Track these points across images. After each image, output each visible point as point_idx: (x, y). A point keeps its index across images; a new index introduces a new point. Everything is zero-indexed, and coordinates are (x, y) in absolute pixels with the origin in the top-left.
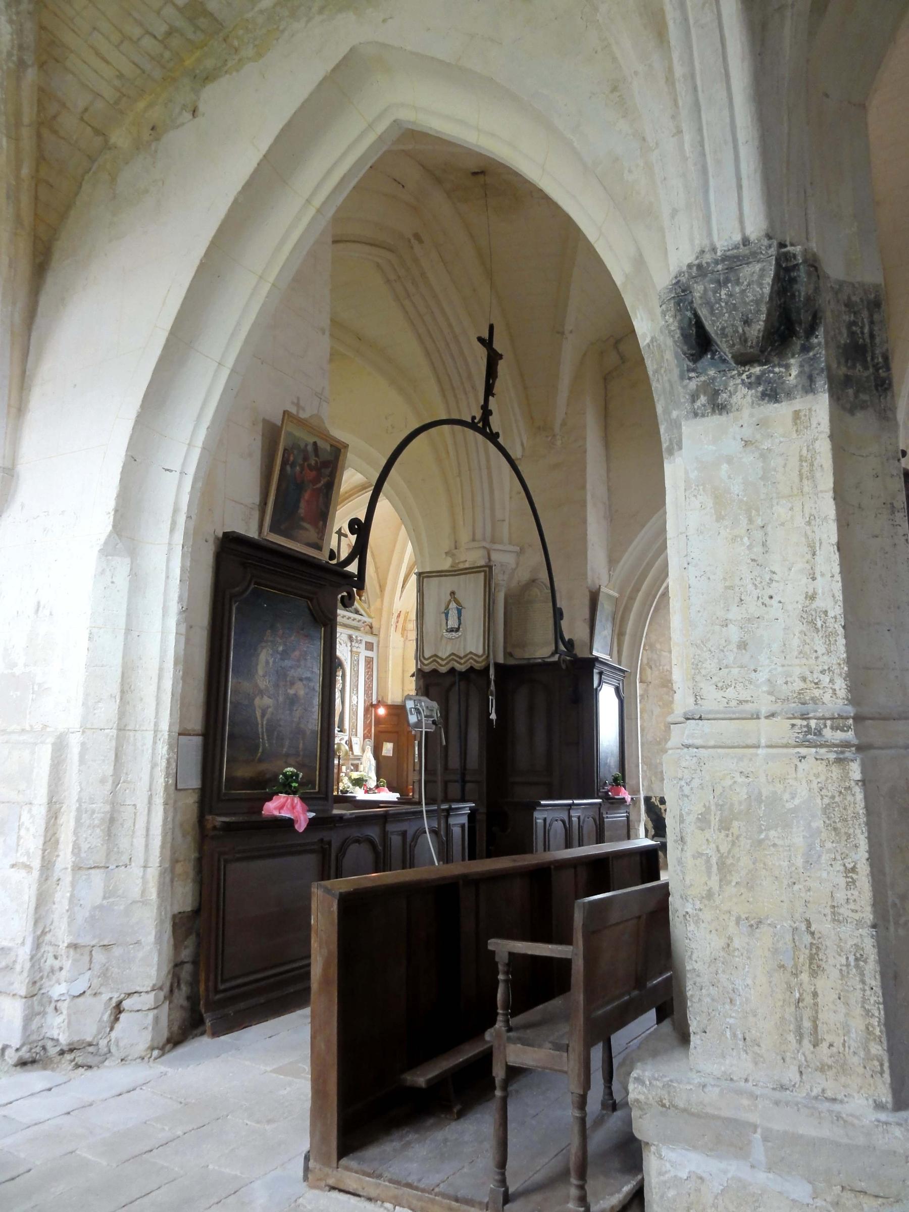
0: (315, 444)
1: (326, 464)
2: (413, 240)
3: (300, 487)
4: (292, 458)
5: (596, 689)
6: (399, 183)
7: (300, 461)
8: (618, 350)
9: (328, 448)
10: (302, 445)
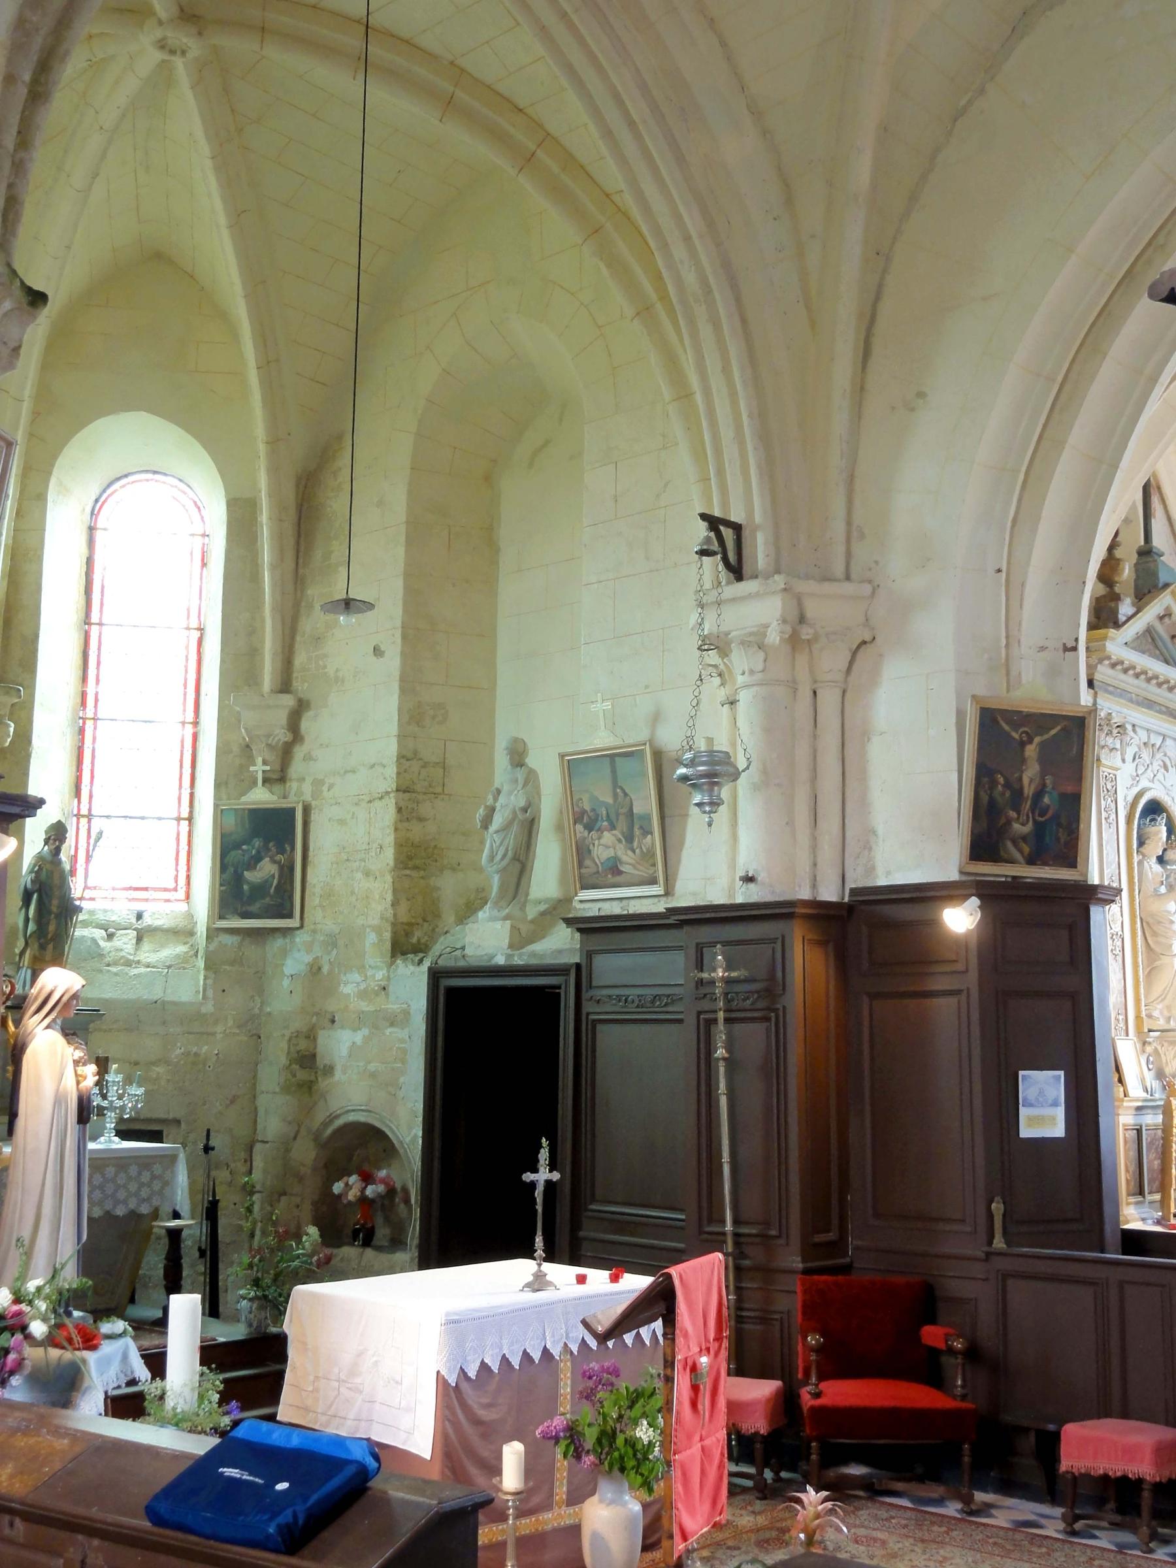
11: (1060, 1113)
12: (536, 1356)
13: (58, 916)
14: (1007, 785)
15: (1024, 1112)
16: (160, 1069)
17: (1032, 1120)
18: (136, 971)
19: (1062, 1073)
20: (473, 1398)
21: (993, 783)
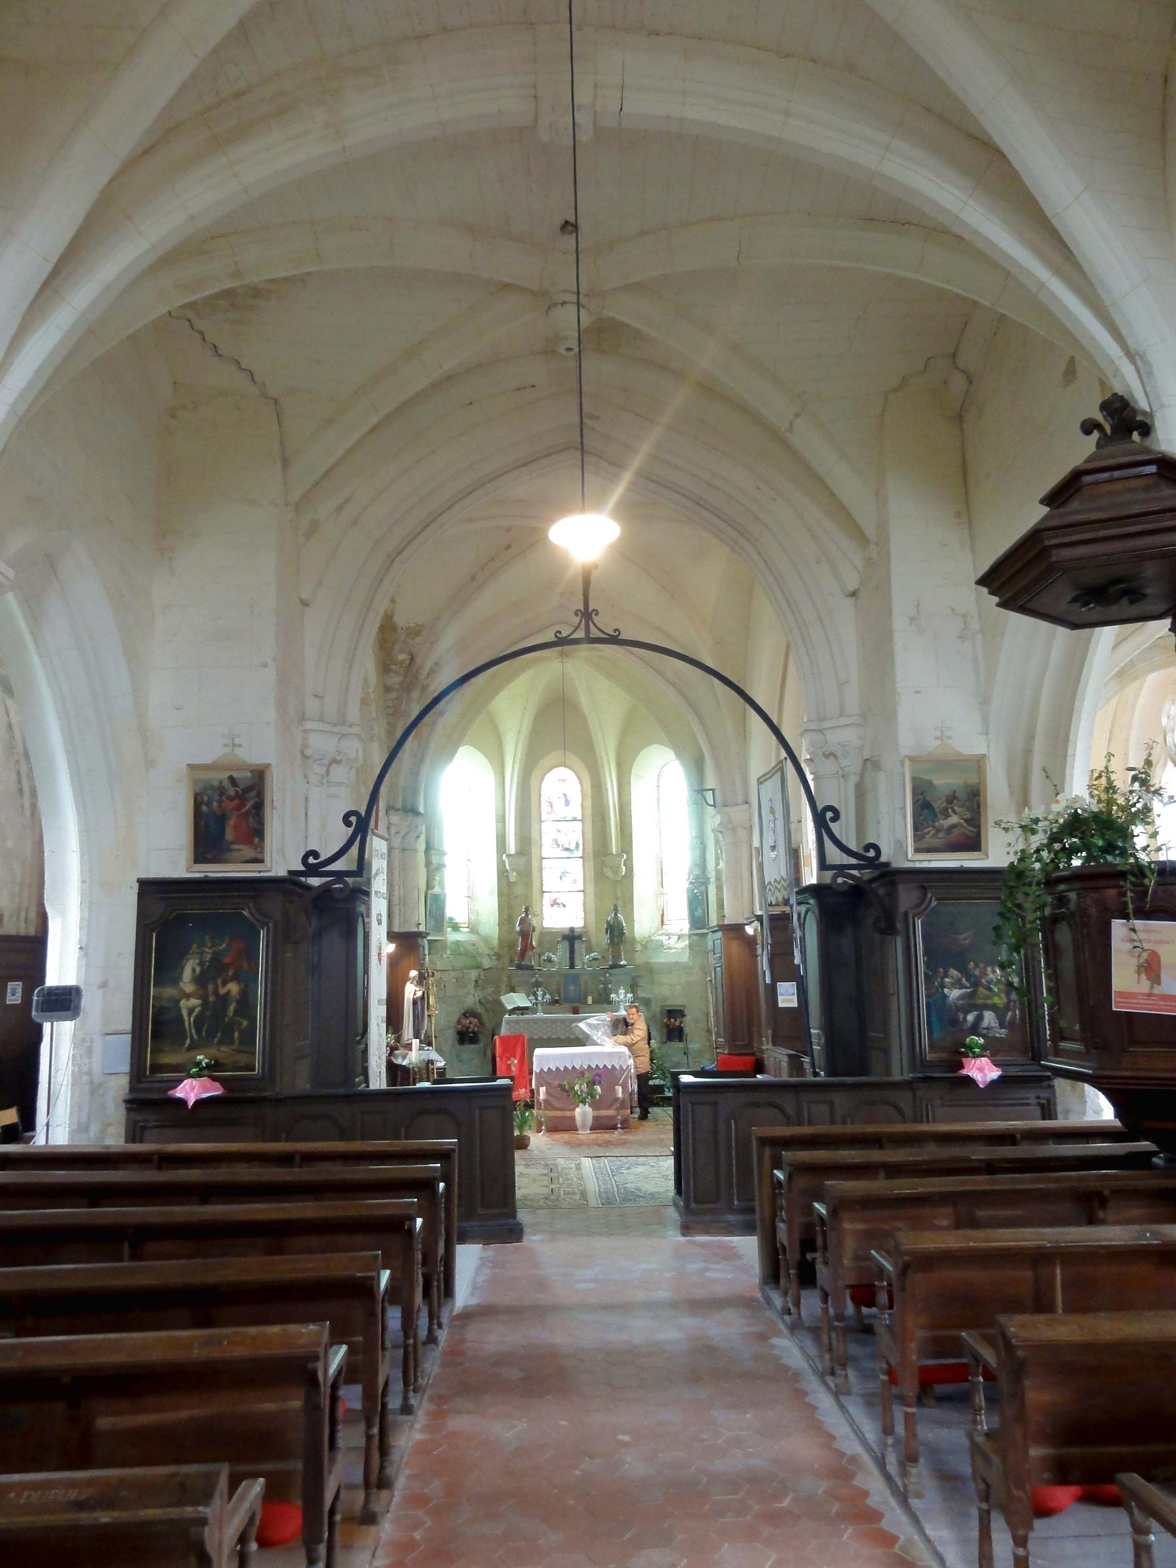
1: (249, 789)
3: (222, 819)
4: (206, 799)
5: (906, 914)
6: (525, 388)
7: (217, 797)
8: (958, 368)
9: (249, 775)
10: (216, 784)
15: (780, 998)
16: (678, 987)
17: (783, 1001)
20: (545, 1076)
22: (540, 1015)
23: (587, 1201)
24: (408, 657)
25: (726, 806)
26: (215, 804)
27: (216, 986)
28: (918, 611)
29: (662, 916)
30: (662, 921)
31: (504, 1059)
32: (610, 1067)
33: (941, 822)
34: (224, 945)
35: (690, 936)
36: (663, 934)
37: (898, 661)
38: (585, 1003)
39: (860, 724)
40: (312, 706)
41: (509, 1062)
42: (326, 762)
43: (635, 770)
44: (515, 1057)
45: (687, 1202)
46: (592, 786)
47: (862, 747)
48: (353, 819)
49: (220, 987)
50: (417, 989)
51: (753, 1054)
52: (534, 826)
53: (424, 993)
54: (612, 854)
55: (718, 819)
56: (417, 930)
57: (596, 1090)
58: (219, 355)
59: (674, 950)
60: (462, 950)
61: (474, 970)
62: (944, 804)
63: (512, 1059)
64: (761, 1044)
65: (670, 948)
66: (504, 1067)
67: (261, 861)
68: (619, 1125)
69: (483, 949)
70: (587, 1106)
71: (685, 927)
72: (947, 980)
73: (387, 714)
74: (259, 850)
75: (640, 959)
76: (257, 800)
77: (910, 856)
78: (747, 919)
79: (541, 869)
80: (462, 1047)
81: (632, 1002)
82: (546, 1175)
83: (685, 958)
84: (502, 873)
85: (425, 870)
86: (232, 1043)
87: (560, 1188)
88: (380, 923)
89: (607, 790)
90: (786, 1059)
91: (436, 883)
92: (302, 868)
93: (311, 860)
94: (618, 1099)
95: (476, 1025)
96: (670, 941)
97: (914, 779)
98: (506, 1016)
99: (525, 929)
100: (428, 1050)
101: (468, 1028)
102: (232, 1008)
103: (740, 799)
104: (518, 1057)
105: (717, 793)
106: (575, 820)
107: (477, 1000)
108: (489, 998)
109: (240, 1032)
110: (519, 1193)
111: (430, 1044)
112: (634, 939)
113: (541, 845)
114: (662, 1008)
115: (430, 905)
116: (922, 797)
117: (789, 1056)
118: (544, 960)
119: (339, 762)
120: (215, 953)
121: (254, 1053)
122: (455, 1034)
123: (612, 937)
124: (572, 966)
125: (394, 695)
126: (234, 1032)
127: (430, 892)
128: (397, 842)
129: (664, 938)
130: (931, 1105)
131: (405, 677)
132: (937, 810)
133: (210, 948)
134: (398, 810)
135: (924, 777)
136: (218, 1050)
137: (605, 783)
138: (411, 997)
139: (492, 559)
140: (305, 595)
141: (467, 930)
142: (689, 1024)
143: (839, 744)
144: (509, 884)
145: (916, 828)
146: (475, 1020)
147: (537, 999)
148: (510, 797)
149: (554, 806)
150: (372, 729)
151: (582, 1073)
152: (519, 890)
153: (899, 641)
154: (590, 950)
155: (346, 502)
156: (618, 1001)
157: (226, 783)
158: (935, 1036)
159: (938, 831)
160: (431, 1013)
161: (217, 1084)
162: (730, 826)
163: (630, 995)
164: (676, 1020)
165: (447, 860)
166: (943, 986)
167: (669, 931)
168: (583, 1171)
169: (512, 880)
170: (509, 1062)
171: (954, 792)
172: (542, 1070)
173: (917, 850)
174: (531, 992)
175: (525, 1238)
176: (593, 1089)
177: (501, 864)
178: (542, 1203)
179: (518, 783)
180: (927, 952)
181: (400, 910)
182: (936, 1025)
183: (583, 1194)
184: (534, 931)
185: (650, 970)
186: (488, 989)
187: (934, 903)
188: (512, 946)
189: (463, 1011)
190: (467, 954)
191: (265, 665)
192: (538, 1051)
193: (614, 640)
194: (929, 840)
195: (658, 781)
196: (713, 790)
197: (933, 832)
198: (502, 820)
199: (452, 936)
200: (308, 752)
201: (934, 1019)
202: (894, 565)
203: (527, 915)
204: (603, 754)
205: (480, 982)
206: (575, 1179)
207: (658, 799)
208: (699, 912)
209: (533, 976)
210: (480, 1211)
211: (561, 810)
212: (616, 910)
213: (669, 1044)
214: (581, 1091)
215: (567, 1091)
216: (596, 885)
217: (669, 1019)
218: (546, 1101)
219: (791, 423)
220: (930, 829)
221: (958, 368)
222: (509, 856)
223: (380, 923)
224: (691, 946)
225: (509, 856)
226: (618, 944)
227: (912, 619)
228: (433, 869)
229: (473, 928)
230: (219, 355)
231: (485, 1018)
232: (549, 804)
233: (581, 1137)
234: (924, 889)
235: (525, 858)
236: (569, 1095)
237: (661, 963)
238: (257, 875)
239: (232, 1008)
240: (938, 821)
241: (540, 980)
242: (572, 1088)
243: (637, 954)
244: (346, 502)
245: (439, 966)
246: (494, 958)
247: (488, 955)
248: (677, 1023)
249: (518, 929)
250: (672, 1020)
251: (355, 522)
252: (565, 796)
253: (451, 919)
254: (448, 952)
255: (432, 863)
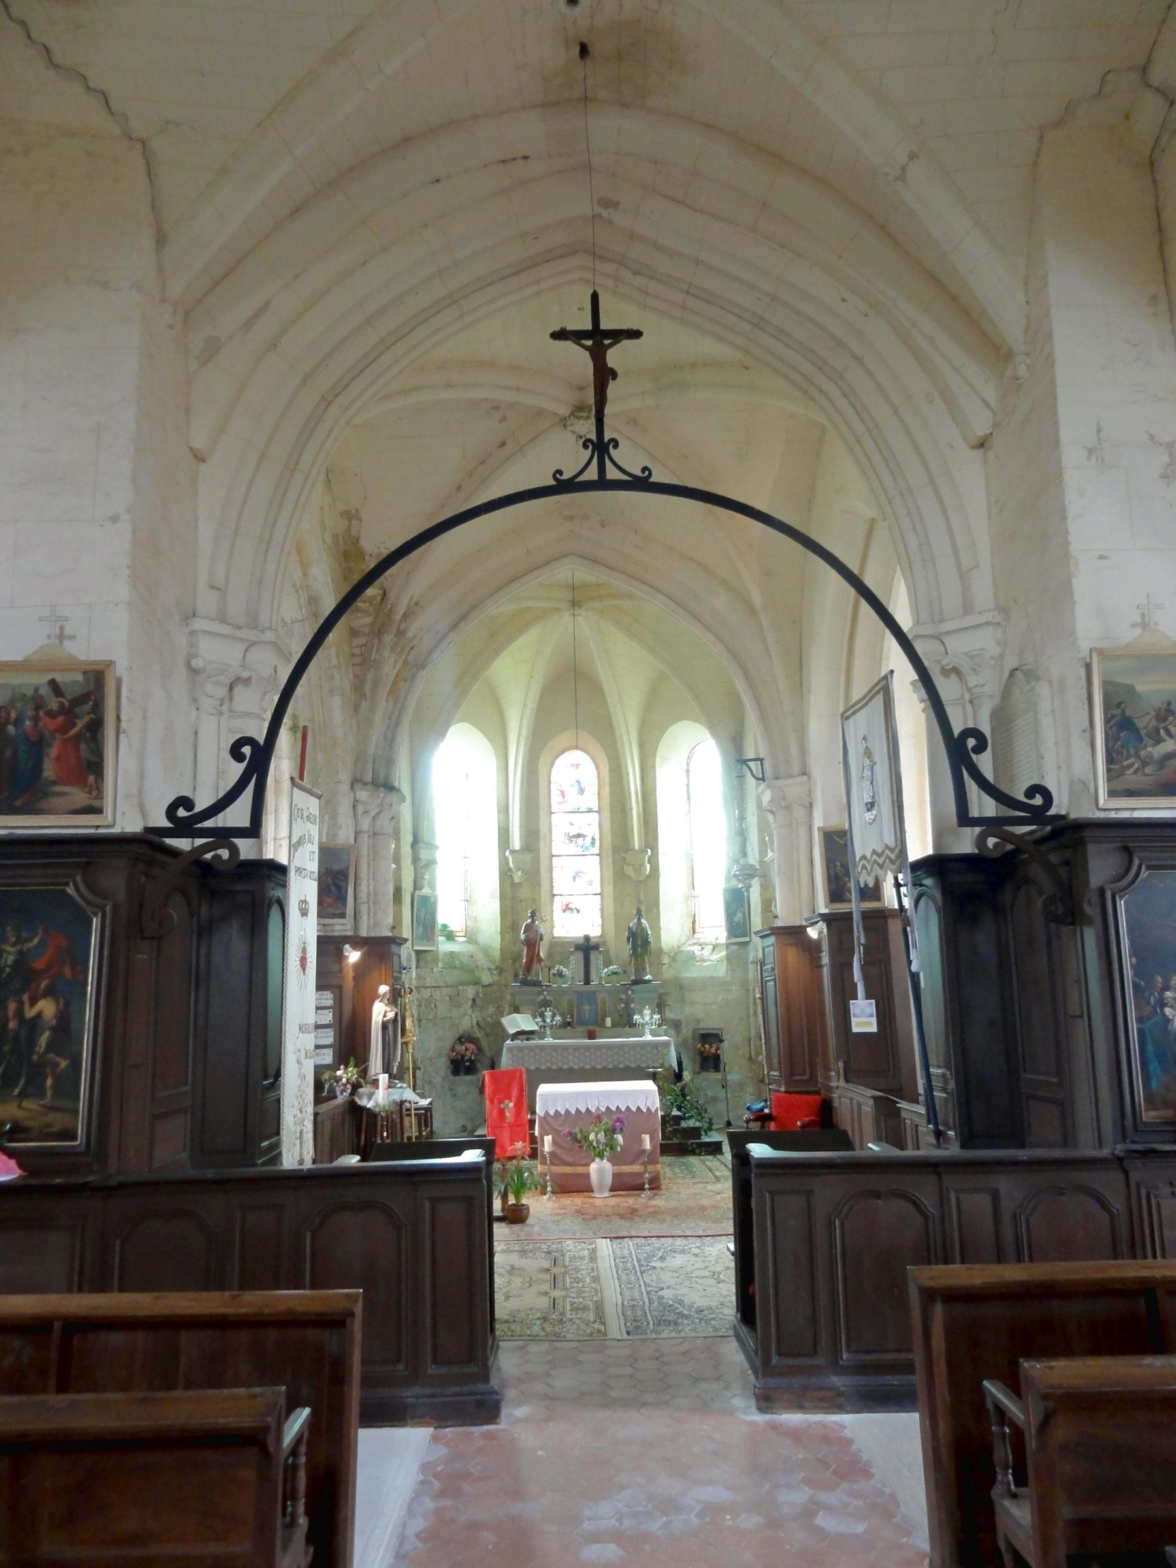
0: (53, 683)
2: (605, 213)
4: (13, 715)
5: (1102, 891)
6: (514, 159)
7: (30, 713)
8: (1149, 86)
9: (80, 678)
10: (29, 692)
11: (874, 1020)
12: (583, 1110)
13: (641, 947)
14: (842, 866)
15: (854, 1020)
16: (714, 1007)
17: (858, 1024)
18: (706, 964)
19: (873, 1001)
20: (551, 1122)
21: (835, 866)
22: (549, 1040)
23: (604, 1324)
24: (381, 592)
25: (777, 778)
26: (28, 723)
27: (21, 1003)
28: (1099, 439)
29: (694, 922)
30: (694, 929)
31: (496, 1101)
32: (634, 1109)
33: (1150, 749)
34: (36, 941)
35: (728, 945)
36: (694, 944)
37: (1072, 510)
38: (603, 1025)
39: (998, 624)
40: (207, 601)
41: (502, 1106)
42: (226, 680)
43: (661, 751)
44: (510, 1099)
45: (766, 1360)
46: (611, 771)
47: (1001, 656)
48: (247, 750)
49: (27, 1007)
50: (388, 1009)
51: (817, 1093)
52: (543, 818)
53: (396, 1014)
54: (633, 849)
55: (767, 797)
56: (390, 934)
57: (616, 1140)
58: (56, 66)
59: (709, 963)
60: (457, 962)
61: (472, 987)
62: (1154, 723)
63: (506, 1102)
64: (829, 1078)
65: (704, 961)
66: (495, 1113)
67: (98, 811)
68: (647, 1186)
69: (482, 961)
70: (605, 1161)
71: (722, 936)
72: (1168, 994)
73: (354, 665)
74: (94, 793)
75: (667, 973)
76: (92, 716)
77: (1101, 802)
78: (806, 920)
79: (551, 870)
80: (457, 1078)
81: (660, 1025)
82: (547, 1270)
83: (722, 971)
84: (505, 874)
85: (412, 868)
86: (41, 1093)
87: (565, 1297)
88: (304, 913)
89: (628, 774)
90: (871, 1102)
91: (426, 882)
92: (166, 823)
93: (182, 813)
94: (644, 1151)
95: (473, 1053)
96: (703, 952)
97: (1105, 684)
98: (508, 1042)
99: (531, 937)
100: (401, 1087)
101: (463, 1056)
102: (44, 1039)
103: (796, 769)
104: (514, 1099)
105: (767, 765)
106: (590, 811)
107: (474, 1023)
108: (489, 1019)
109: (57, 1079)
110: (502, 1308)
111: (401, 1079)
112: (660, 950)
113: (551, 841)
114: (695, 1030)
115: (418, 910)
116: (1119, 711)
117: (875, 1098)
118: (554, 974)
119: (247, 681)
120: (21, 953)
121: (76, 1112)
122: (449, 1062)
123: (634, 947)
124: (587, 981)
125: (362, 640)
126: (46, 1078)
127: (417, 893)
128: (365, 824)
129: (696, 949)
130: (1156, 1196)
131: (376, 617)
132: (1143, 732)
133: (14, 945)
134: (365, 784)
135: (1125, 680)
136: (20, 1107)
137: (626, 768)
138: (380, 1018)
139: (483, 462)
140: (199, 441)
141: (464, 939)
142: (727, 1052)
143: (966, 654)
144: (514, 885)
145: (1110, 760)
146: (471, 1047)
147: (544, 1021)
148: (514, 783)
149: (566, 794)
150: (332, 678)
151: (599, 1118)
152: (524, 893)
153: (1072, 480)
154: (608, 963)
155: (257, 315)
156: (643, 1024)
157: (45, 691)
158: (1154, 1084)
159: (1145, 764)
160: (408, 1039)
161: (12, 1163)
162: (783, 804)
163: (657, 1017)
164: (711, 1047)
165: (439, 856)
166: (1162, 1004)
167: (702, 941)
168: (600, 1265)
169: (517, 880)
170: (502, 1106)
171: (1169, 704)
172: (547, 1113)
173: (1112, 793)
174: (538, 1011)
175: (505, 1411)
176: (612, 1139)
177: (503, 861)
178: (536, 1329)
179: (523, 767)
180: (1134, 952)
181: (369, 908)
182: (1154, 1067)
183: (599, 1309)
184: (541, 939)
185: (680, 986)
186: (488, 1009)
187: (1144, 874)
188: (516, 958)
189: (457, 1036)
190: (463, 967)
191: (115, 519)
192: (544, 1089)
193: (641, 483)
194: (1131, 778)
195: (688, 765)
196: (761, 760)
197: (1136, 766)
198: (504, 810)
199: (444, 947)
200: (194, 663)
201: (1150, 1056)
202: (1062, 374)
203: (533, 921)
204: (623, 730)
205: (478, 1001)
206: (588, 1280)
207: (688, 785)
208: (739, 916)
209: (540, 993)
210: (432, 1370)
211: (574, 800)
212: (639, 914)
213: (705, 1074)
214: (598, 1142)
215: (580, 1142)
216: (615, 885)
217: (703, 1046)
218: (552, 1154)
219: (903, 168)
220: (1132, 760)
221: (1149, 86)
222: (512, 852)
223: (304, 913)
224: (728, 958)
225: (512, 852)
226: (642, 956)
227: (1090, 451)
228: (422, 866)
229: (471, 938)
230: (56, 66)
231: (484, 1043)
232: (559, 793)
233: (598, 1202)
234: (1128, 851)
235: (531, 855)
236: (581, 1147)
237: (694, 979)
238: (92, 831)
239: (44, 1039)
240: (1145, 747)
241: (548, 998)
242: (586, 1138)
243: (664, 967)
244: (257, 315)
245: (429, 981)
246: (495, 972)
247: (489, 969)
248: (713, 1050)
249: (522, 937)
250: (707, 1046)
251: (273, 345)
252: (579, 782)
253: (445, 926)
254: (440, 965)
255: (420, 859)
